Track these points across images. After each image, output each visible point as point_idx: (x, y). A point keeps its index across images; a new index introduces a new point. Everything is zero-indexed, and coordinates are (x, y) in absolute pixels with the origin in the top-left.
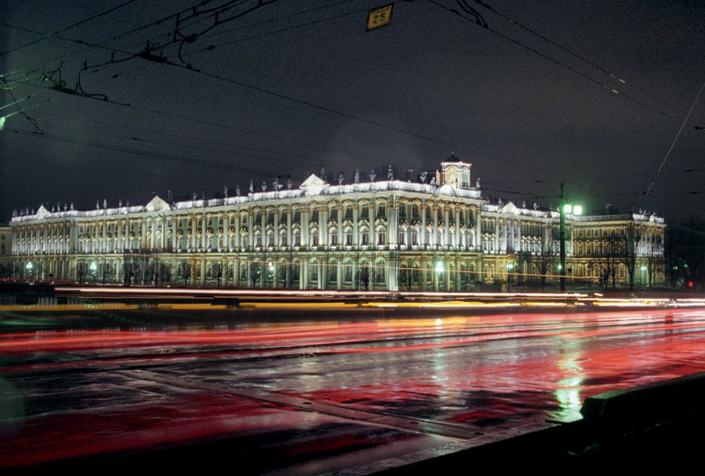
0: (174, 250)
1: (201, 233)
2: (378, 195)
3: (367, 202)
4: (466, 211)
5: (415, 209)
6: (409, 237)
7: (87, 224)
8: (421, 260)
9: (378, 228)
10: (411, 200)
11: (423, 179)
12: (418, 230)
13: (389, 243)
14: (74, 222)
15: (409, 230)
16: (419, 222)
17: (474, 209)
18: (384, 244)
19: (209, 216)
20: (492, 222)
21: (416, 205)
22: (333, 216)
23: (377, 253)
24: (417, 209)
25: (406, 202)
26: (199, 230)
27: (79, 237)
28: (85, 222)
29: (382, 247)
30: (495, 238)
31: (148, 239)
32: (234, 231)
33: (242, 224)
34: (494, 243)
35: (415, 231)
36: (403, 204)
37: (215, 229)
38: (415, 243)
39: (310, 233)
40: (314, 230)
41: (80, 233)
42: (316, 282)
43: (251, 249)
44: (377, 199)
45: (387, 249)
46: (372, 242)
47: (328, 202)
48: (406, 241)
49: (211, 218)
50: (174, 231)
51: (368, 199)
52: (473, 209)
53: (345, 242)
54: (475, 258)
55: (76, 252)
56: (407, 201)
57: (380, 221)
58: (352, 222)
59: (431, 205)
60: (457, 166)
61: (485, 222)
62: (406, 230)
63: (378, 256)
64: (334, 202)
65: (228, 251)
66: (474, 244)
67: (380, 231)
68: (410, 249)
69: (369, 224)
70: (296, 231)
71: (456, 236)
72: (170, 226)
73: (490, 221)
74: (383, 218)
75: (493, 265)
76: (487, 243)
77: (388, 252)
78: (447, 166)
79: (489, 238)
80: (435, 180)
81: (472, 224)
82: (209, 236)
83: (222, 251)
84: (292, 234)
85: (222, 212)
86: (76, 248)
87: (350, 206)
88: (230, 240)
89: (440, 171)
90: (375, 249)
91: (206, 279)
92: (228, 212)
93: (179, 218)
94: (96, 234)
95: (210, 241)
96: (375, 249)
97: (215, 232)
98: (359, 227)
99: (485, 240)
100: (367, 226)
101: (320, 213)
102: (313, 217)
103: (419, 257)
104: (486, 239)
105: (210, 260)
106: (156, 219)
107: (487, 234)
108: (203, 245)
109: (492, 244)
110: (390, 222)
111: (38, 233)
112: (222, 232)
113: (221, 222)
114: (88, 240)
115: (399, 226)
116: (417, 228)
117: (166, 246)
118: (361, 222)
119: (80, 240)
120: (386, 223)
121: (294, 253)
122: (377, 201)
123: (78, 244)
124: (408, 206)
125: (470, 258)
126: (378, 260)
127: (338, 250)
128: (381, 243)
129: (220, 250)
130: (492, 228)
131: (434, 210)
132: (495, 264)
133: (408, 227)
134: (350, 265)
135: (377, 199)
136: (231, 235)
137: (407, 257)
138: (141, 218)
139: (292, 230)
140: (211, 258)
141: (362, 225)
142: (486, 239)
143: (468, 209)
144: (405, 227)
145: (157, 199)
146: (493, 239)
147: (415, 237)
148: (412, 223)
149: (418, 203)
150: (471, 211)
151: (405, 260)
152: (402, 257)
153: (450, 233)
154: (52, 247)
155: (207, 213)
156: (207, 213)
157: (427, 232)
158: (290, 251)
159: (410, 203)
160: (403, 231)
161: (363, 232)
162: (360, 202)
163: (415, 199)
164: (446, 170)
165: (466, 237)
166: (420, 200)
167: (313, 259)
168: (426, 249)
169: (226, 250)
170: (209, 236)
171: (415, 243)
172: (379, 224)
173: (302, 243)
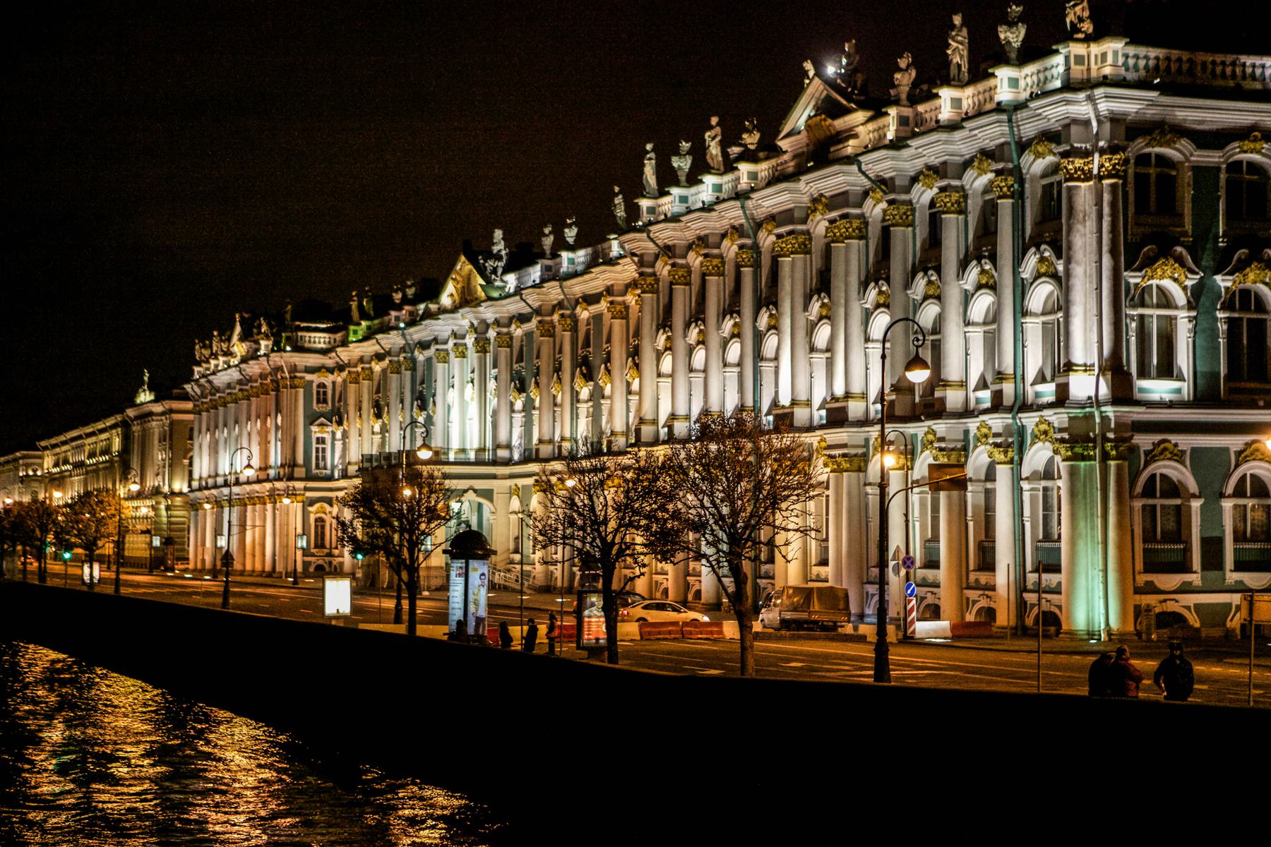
14: (293, 369)
35: (1245, 300)
36: (1162, 160)
44: (1023, 146)
45: (1062, 398)
48: (1183, 360)
56: (1184, 144)
62: (1180, 297)
77: (1058, 418)
110: (1068, 262)
115: (1133, 278)
124: (1198, 170)
134: (989, 485)
135: (1023, 146)
137: (1186, 442)
145: (463, 266)
151: (1178, 456)
160: (1166, 301)
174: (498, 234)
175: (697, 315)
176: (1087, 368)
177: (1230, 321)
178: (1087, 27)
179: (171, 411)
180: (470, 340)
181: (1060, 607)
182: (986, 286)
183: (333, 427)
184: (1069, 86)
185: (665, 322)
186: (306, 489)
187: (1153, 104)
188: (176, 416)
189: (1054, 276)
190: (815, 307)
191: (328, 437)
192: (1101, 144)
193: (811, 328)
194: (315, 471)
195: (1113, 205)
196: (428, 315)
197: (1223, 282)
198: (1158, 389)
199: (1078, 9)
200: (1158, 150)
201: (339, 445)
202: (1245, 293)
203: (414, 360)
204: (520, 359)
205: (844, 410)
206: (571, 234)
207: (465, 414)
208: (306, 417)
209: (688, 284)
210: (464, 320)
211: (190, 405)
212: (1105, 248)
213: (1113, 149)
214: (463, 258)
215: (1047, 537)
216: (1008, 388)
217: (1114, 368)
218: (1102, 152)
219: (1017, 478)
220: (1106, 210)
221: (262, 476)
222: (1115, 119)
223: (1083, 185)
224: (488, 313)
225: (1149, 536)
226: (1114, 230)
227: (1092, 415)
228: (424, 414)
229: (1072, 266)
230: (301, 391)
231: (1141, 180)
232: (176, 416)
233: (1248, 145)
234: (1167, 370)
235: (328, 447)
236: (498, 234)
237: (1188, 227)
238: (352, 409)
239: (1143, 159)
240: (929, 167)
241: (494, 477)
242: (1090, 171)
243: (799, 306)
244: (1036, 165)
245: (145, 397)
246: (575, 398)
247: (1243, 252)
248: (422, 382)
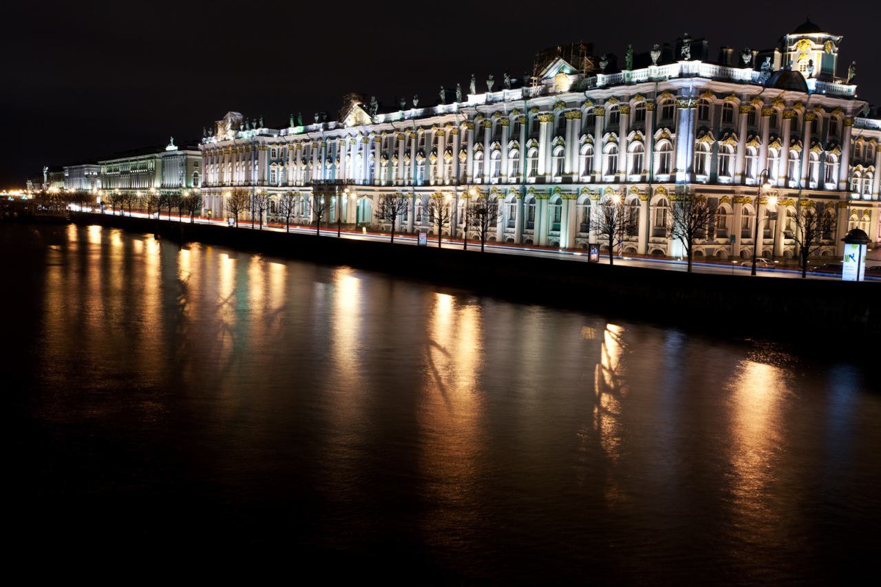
0: (377, 182)
1: (409, 157)
2: (662, 87)
3: (644, 100)
4: (825, 119)
5: (728, 114)
6: (714, 159)
7: (281, 147)
8: (734, 201)
9: (659, 146)
10: (722, 95)
11: (747, 59)
12: (732, 150)
13: (675, 170)
14: (264, 143)
15: (715, 148)
16: (734, 134)
17: (839, 116)
18: (667, 173)
19: (420, 132)
20: (870, 147)
21: (731, 106)
22: (589, 127)
23: (654, 186)
24: (731, 112)
25: (712, 99)
26: (408, 152)
27: (270, 163)
28: (278, 144)
29: (664, 177)
30: (874, 173)
31: (347, 167)
32: (451, 154)
34: (871, 181)
35: (725, 150)
36: (706, 102)
37: (428, 151)
38: (725, 173)
39: (553, 155)
40: (559, 149)
41: (272, 158)
42: (557, 233)
43: (469, 180)
44: (659, 93)
45: (672, 180)
46: (648, 168)
47: (582, 103)
48: (707, 169)
49: (423, 135)
50: (378, 153)
51: (644, 95)
52: (838, 116)
53: (606, 168)
54: (835, 201)
55: (266, 183)
56: (714, 97)
57: (664, 133)
59: (758, 106)
60: (814, 40)
61: (858, 146)
62: (708, 147)
63: (656, 192)
64: (590, 103)
65: (443, 184)
66: (835, 177)
67: (664, 149)
68: (714, 180)
69: (644, 138)
70: (532, 152)
71: (801, 163)
72: (373, 148)
73: (867, 143)
74: (669, 128)
75: (867, 217)
76: (859, 180)
77: (672, 186)
78: (796, 40)
79: (863, 173)
80: (772, 62)
81: (834, 143)
82: (420, 163)
83: (436, 184)
84: (526, 156)
85: (437, 125)
86: (266, 178)
87: (616, 108)
88: (447, 166)
89: (783, 51)
90: (652, 181)
91: (413, 224)
92: (445, 125)
93: (384, 136)
94: (314, 159)
95: (422, 170)
96: (652, 181)
97: (427, 156)
98: (628, 144)
99: (856, 176)
100: (641, 141)
101: (569, 121)
102: (558, 129)
103: (730, 196)
104: (858, 174)
105: (420, 197)
106: (357, 138)
107: (861, 167)
108: (412, 176)
109: (867, 183)
110: (678, 134)
111: (227, 157)
112: (436, 156)
113: (436, 141)
115: (697, 141)
116: (729, 145)
117: (368, 178)
118: (632, 134)
119: (272, 167)
120: (673, 136)
121: (528, 187)
122: (660, 97)
123: (269, 173)
124: (718, 107)
125: (826, 201)
126: (656, 199)
127: (593, 181)
128: (663, 170)
129: (432, 183)
130: (870, 155)
131: (763, 115)
132: (870, 216)
133: (712, 142)
135: (659, 93)
136: (448, 161)
140: (422, 193)
141: (634, 140)
142: (858, 174)
143: (829, 115)
144: (707, 143)
146: (870, 175)
147: (725, 162)
148: (721, 137)
149: (735, 102)
150: (833, 118)
152: (698, 194)
153: (790, 156)
154: (241, 176)
155: (418, 128)
156: (418, 128)
157: (747, 152)
158: (522, 184)
159: (720, 102)
160: (703, 149)
161: (635, 151)
162: (632, 101)
163: (729, 94)
164: (793, 48)
165: (821, 166)
166: (739, 96)
167: (555, 197)
168: (743, 183)
169: (440, 182)
170: (420, 163)
171: (725, 173)
172: (661, 138)
173: (541, 172)
174: (373, 98)
175: (497, 138)
176: (682, 171)
177: (722, 157)
178: (689, 55)
179: (187, 154)
180: (360, 138)
181: (637, 247)
182: (638, 140)
183: (279, 166)
184: (681, 75)
185: (479, 139)
186: (268, 190)
187: (709, 83)
188: (189, 157)
189: (669, 139)
190: (556, 140)
191: (276, 170)
192: (692, 96)
193: (553, 148)
194: (271, 183)
195: (694, 117)
196: (337, 127)
197: (720, 143)
198: (699, 178)
199: (686, 49)
200: (706, 98)
201: (281, 173)
202: (724, 147)
203: (326, 144)
204: (386, 147)
205: (571, 179)
206: (415, 102)
207: (354, 165)
208: (268, 162)
209: (491, 127)
210: (356, 131)
211: (199, 153)
212: (690, 131)
213: (696, 98)
214: (356, 104)
215: (511, 219)
216: (648, 175)
217: (690, 171)
218: (692, 99)
219: (648, 205)
220: (692, 118)
221: (247, 184)
222: (696, 88)
223: (684, 109)
224: (370, 129)
225: (836, 230)
226: (694, 125)
227: (683, 187)
228: (331, 164)
229: (679, 136)
230: (266, 151)
231: (700, 107)
232: (189, 157)
233: (730, 98)
234: (702, 172)
235: (276, 174)
236: (373, 98)
237: (712, 125)
238: (290, 160)
239: (701, 102)
240: (613, 96)
241: (373, 190)
242: (687, 105)
243: (549, 140)
244: (661, 100)
245: (171, 148)
246: (416, 163)
247: (727, 134)
248: (330, 152)
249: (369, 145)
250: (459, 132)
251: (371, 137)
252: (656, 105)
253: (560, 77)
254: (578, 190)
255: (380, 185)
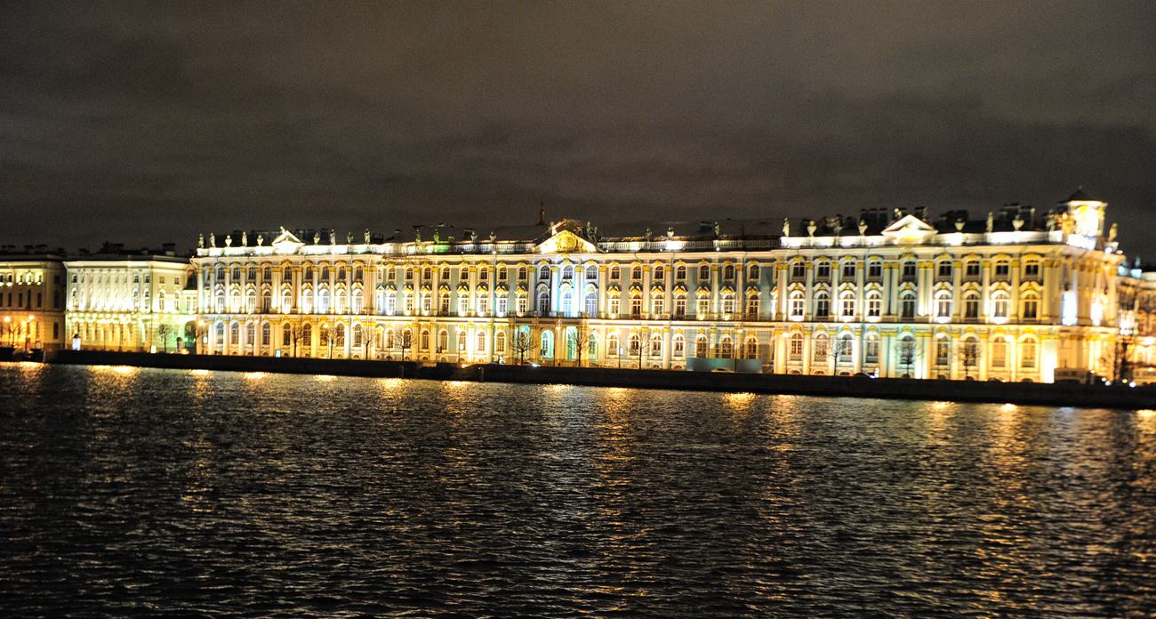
0: (603, 315)
33: (749, 280)
41: (379, 281)
50: (602, 286)
57: (1030, 285)
58: (916, 285)
114: (390, 292)
121: (867, 326)
129: (701, 317)
138: (526, 262)
139: (865, 293)
249: (584, 275)
250: (744, 269)
251: (587, 265)
252: (1020, 263)
253: (910, 230)
254: (933, 329)
255: (607, 318)
